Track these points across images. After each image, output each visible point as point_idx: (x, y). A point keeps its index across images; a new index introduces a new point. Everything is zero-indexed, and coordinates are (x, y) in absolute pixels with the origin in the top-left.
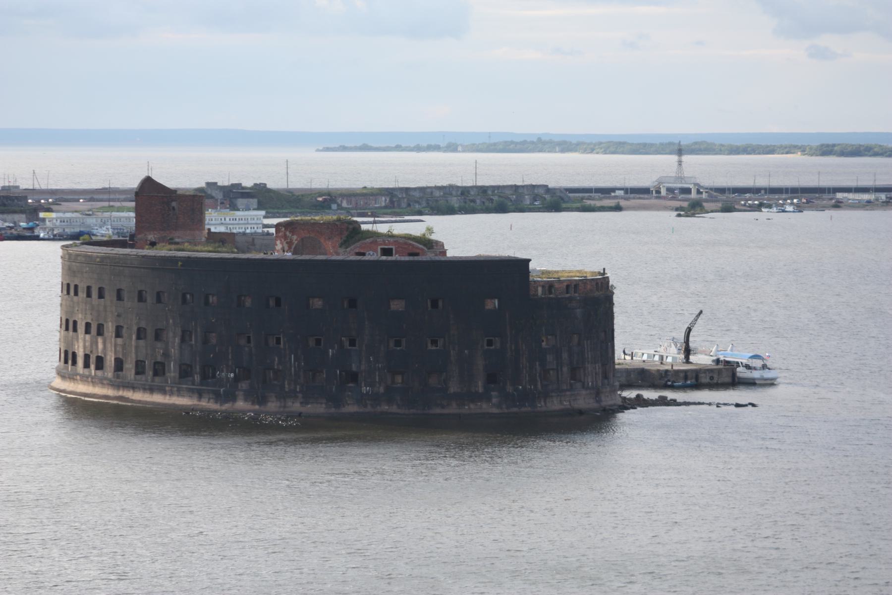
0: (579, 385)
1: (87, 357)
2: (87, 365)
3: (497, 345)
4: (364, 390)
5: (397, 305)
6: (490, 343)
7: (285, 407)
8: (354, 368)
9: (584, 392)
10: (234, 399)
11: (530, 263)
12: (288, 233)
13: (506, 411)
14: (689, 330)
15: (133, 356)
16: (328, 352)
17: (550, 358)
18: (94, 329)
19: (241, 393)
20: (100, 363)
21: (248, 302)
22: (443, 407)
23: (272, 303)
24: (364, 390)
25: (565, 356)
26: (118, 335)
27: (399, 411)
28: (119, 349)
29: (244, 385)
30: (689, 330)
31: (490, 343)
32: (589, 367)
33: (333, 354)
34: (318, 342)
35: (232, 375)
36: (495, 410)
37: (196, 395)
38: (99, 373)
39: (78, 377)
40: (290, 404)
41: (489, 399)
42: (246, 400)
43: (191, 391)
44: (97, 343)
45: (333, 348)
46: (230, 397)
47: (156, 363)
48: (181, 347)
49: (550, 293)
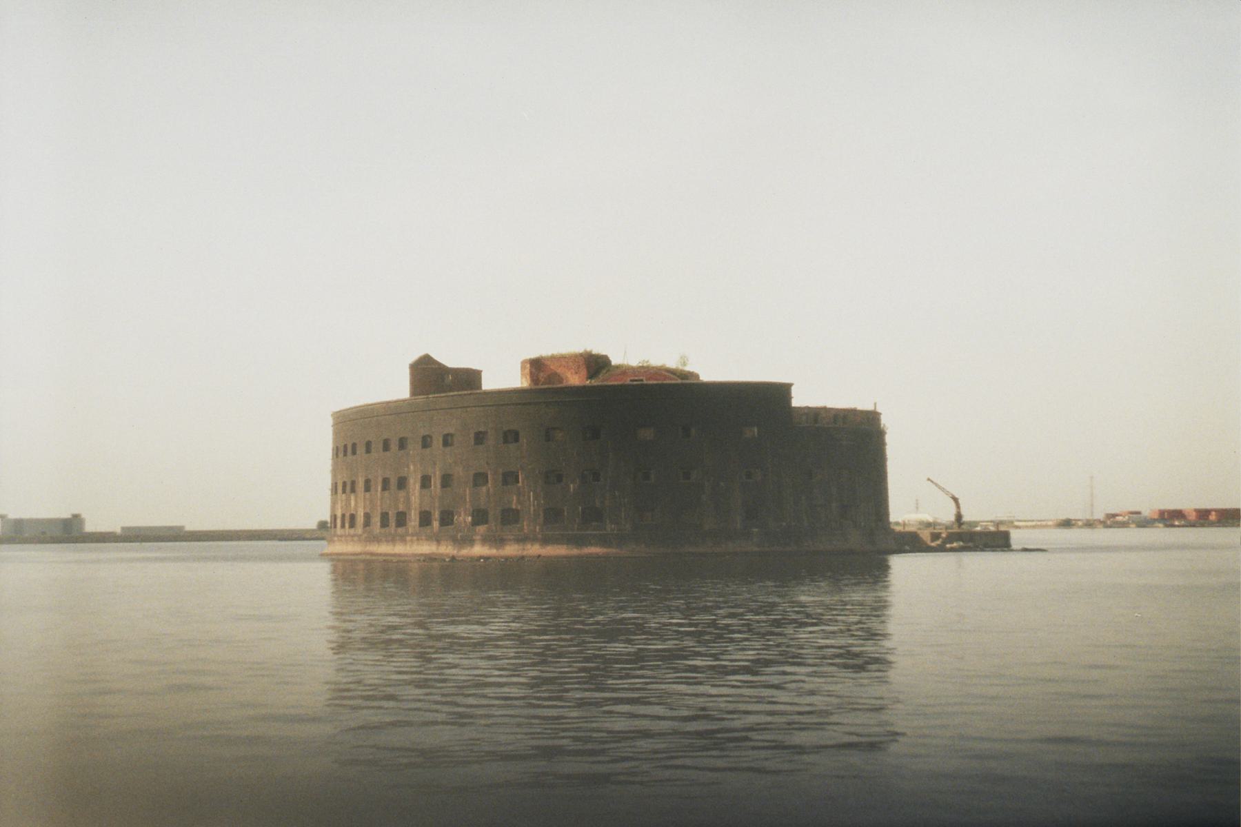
2: (343, 526)
6: (749, 476)
8: (598, 504)
10: (471, 542)
18: (348, 488)
26: (367, 489)
29: (481, 529)
31: (749, 476)
36: (756, 549)
38: (352, 531)
42: (483, 545)
43: (429, 538)
46: (468, 541)
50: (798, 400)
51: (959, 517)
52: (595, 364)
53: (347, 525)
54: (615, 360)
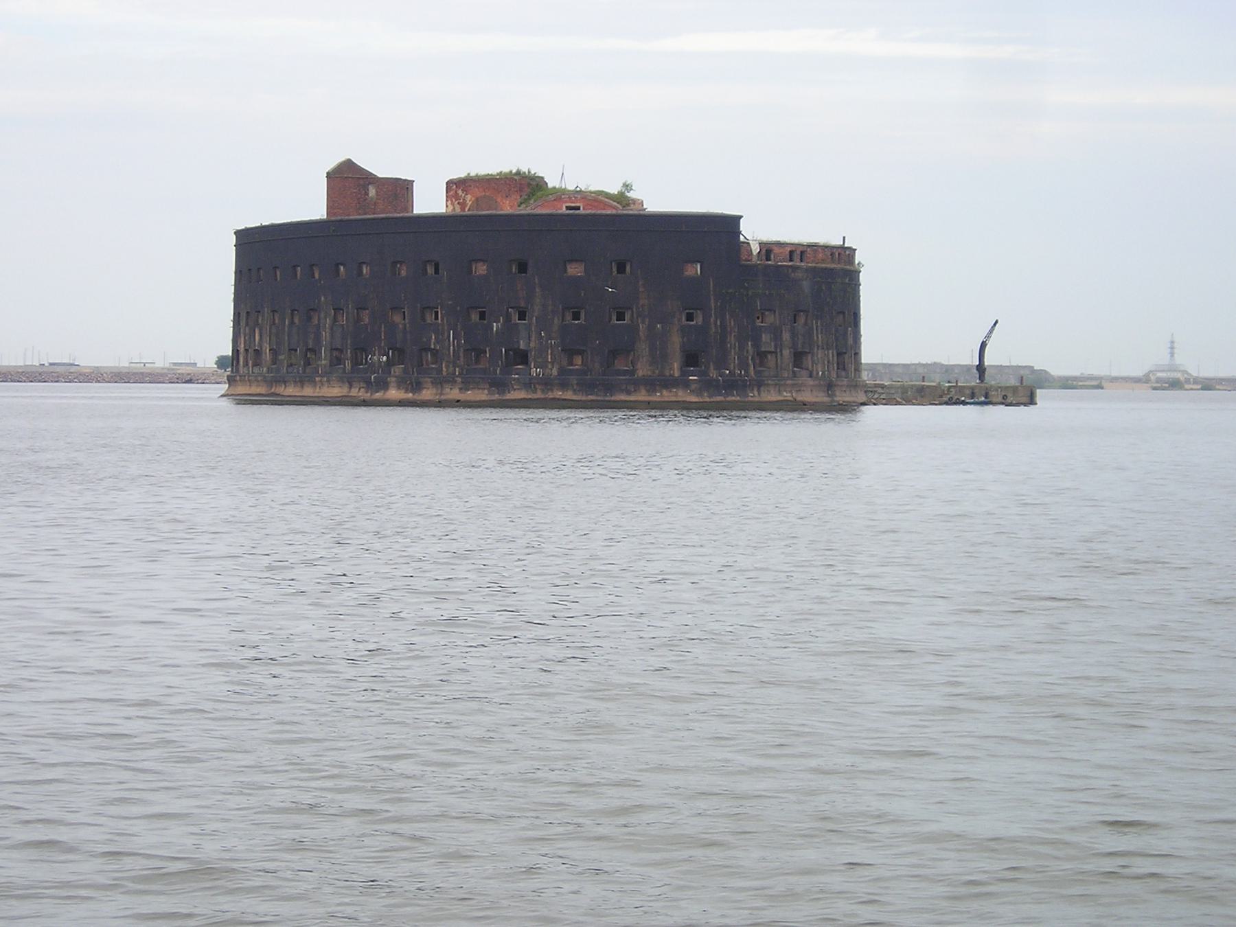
1: (247, 350)
2: (246, 364)
3: (699, 320)
5: (575, 270)
6: (690, 317)
7: (441, 394)
8: (522, 346)
9: (811, 382)
12: (460, 192)
13: (707, 399)
14: (983, 346)
17: (765, 338)
21: (403, 273)
22: (629, 393)
23: (430, 270)
25: (786, 336)
27: (574, 398)
28: (274, 338)
29: (397, 370)
30: (983, 346)
31: (690, 317)
32: (820, 354)
34: (482, 316)
38: (256, 370)
40: (448, 390)
41: (686, 384)
42: (399, 388)
43: (341, 380)
48: (332, 329)
49: (768, 259)
50: (754, 232)
51: (981, 368)
52: (528, 185)
53: (250, 363)
54: (552, 182)
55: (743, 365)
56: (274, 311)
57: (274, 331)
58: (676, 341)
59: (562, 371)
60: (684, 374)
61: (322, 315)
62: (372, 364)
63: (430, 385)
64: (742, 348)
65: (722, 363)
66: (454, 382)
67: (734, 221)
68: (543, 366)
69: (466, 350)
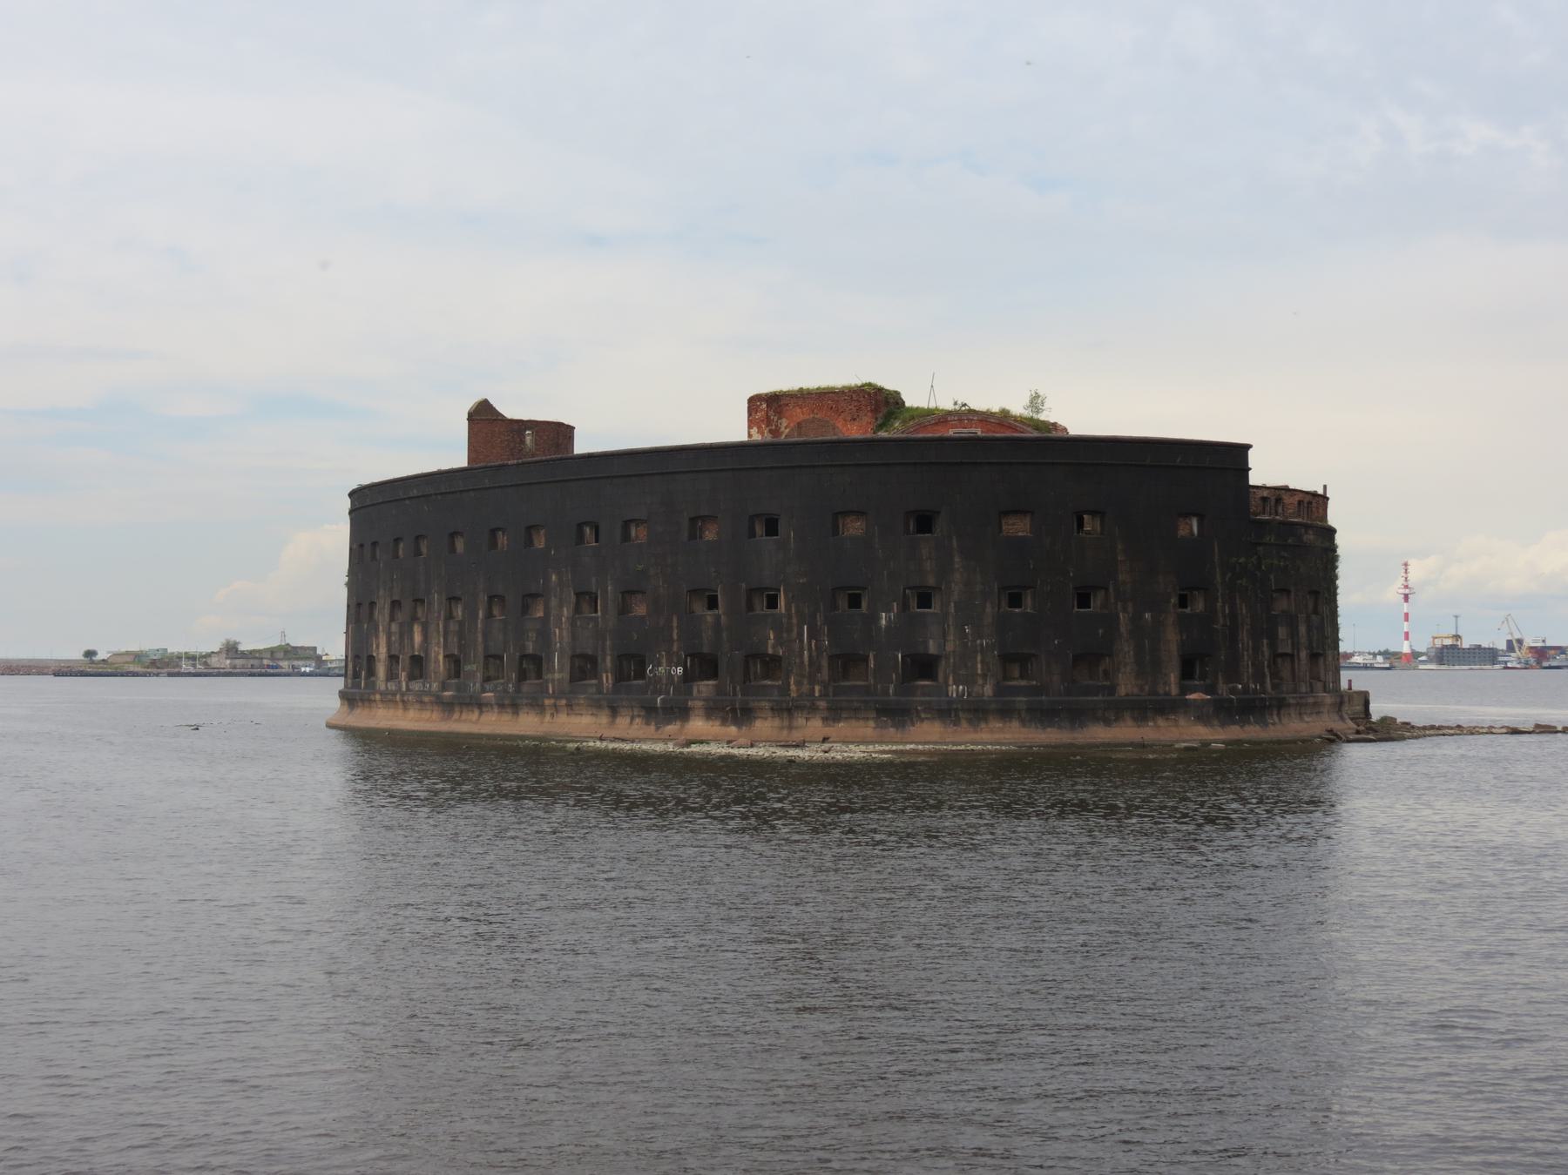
0: (1319, 685)
1: (393, 658)
2: (392, 676)
3: (1199, 606)
4: (953, 690)
7: (790, 728)
8: (932, 648)
11: (1250, 452)
15: (480, 648)
16: (879, 618)
17: (1282, 632)
19: (699, 704)
20: (418, 666)
24: (953, 690)
25: (1303, 629)
29: (705, 687)
33: (889, 620)
35: (680, 670)
37: (607, 711)
38: (416, 686)
39: (378, 697)
43: (596, 705)
44: (411, 631)
45: (888, 611)
46: (678, 711)
47: (523, 657)
48: (573, 623)
52: (882, 402)
54: (914, 398)
55: (1258, 676)
56: (452, 599)
57: (453, 627)
58: (1172, 641)
59: (1000, 691)
60: (1184, 690)
61: (554, 602)
62: (657, 680)
63: (770, 714)
64: (1257, 649)
65: (1233, 674)
66: (813, 709)
67: (1241, 450)
68: (969, 680)
69: (831, 658)
